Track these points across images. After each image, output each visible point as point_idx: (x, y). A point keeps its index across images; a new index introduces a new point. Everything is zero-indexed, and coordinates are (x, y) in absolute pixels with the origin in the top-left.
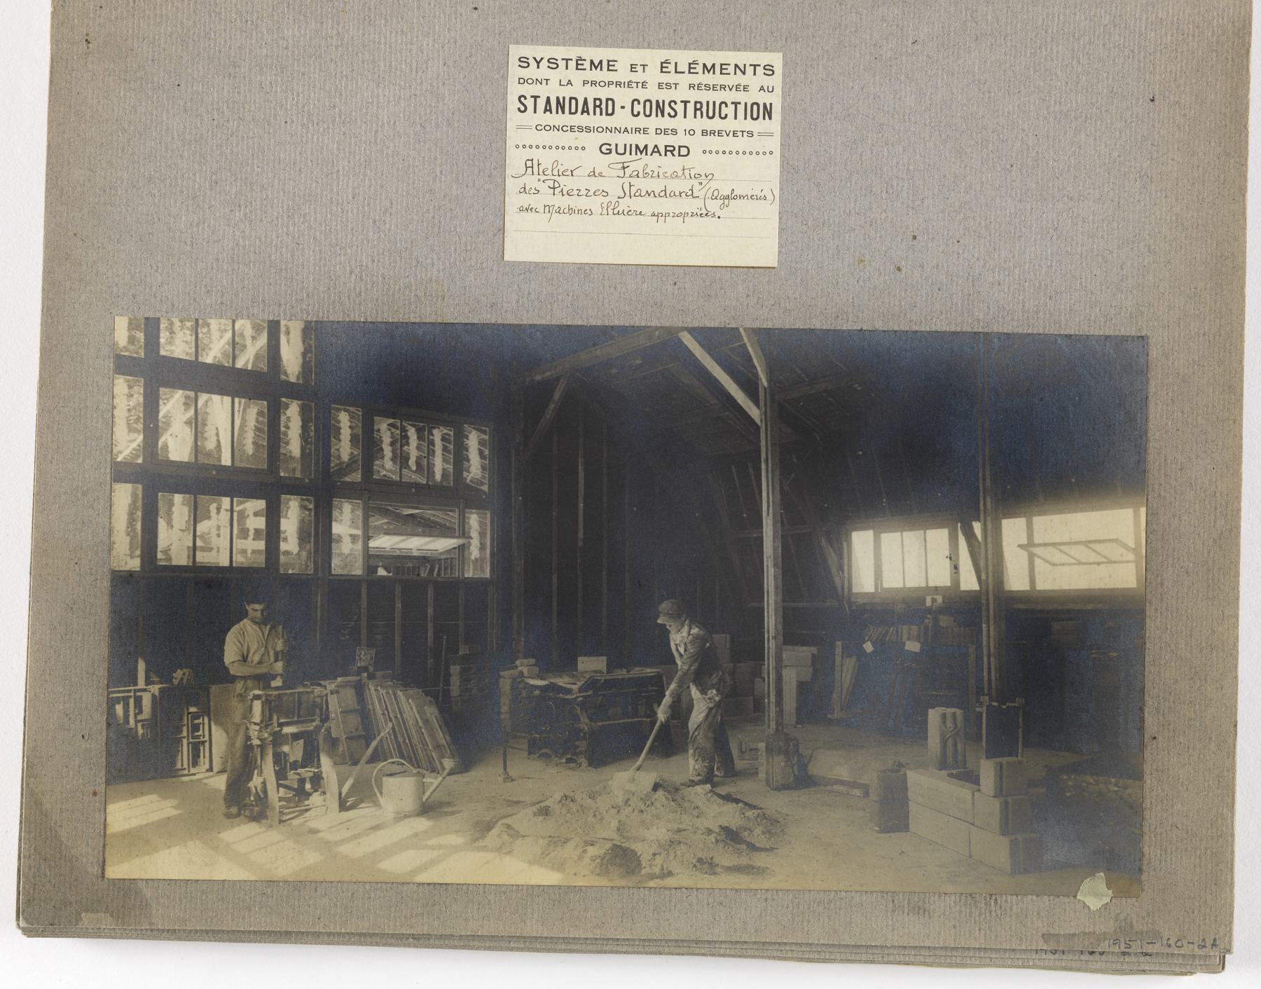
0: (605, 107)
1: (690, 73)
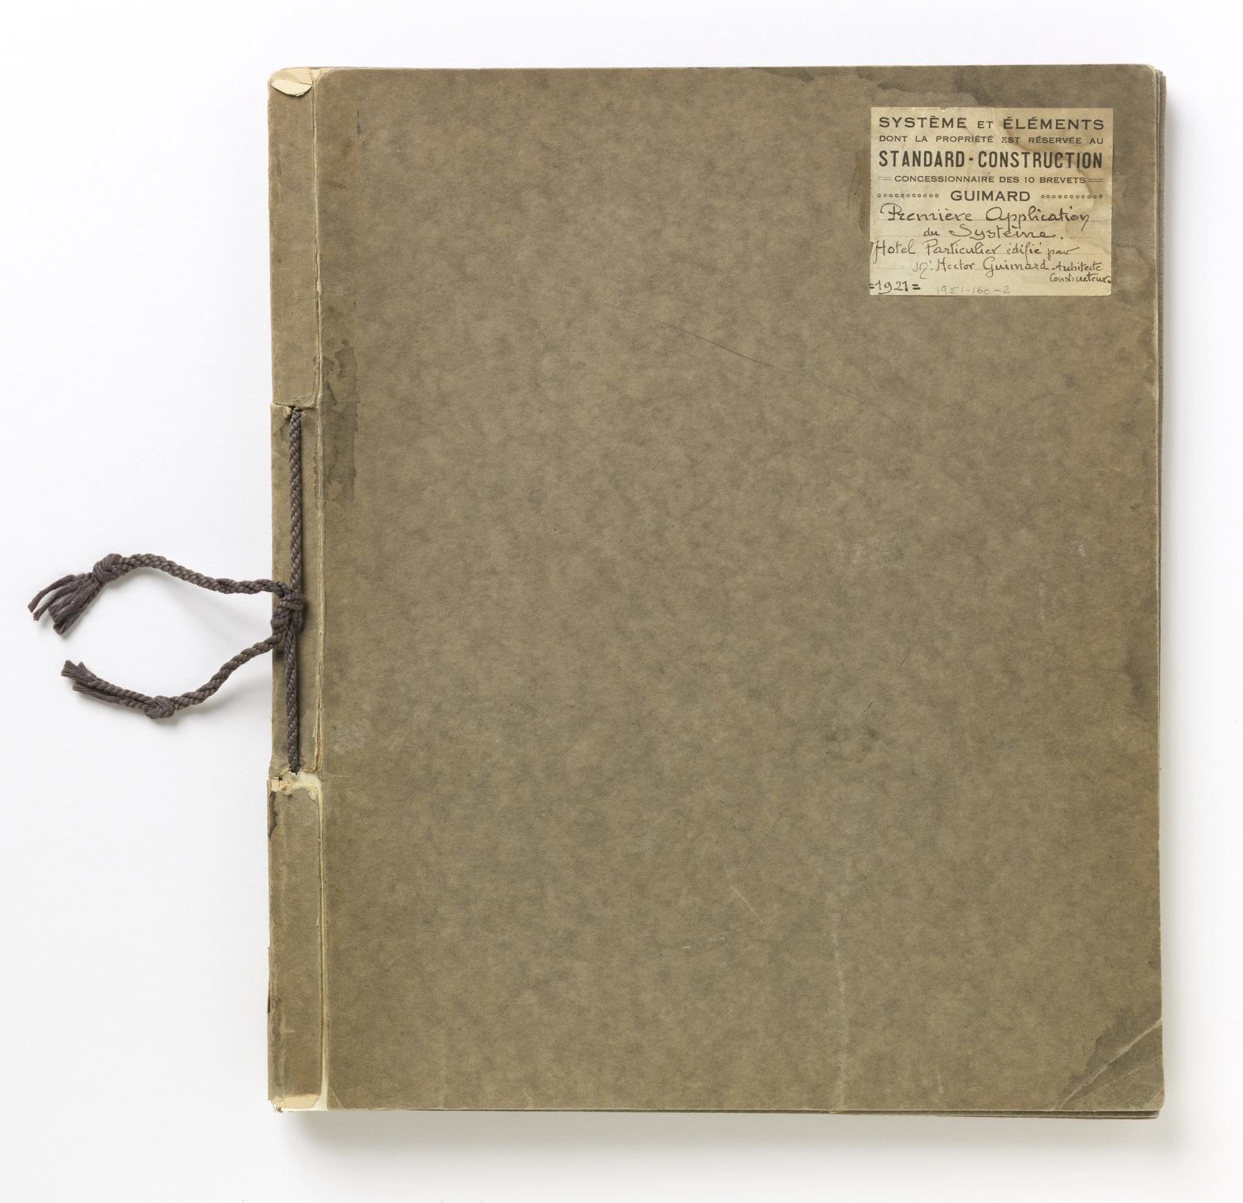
0: (957, 159)
1: (1029, 128)
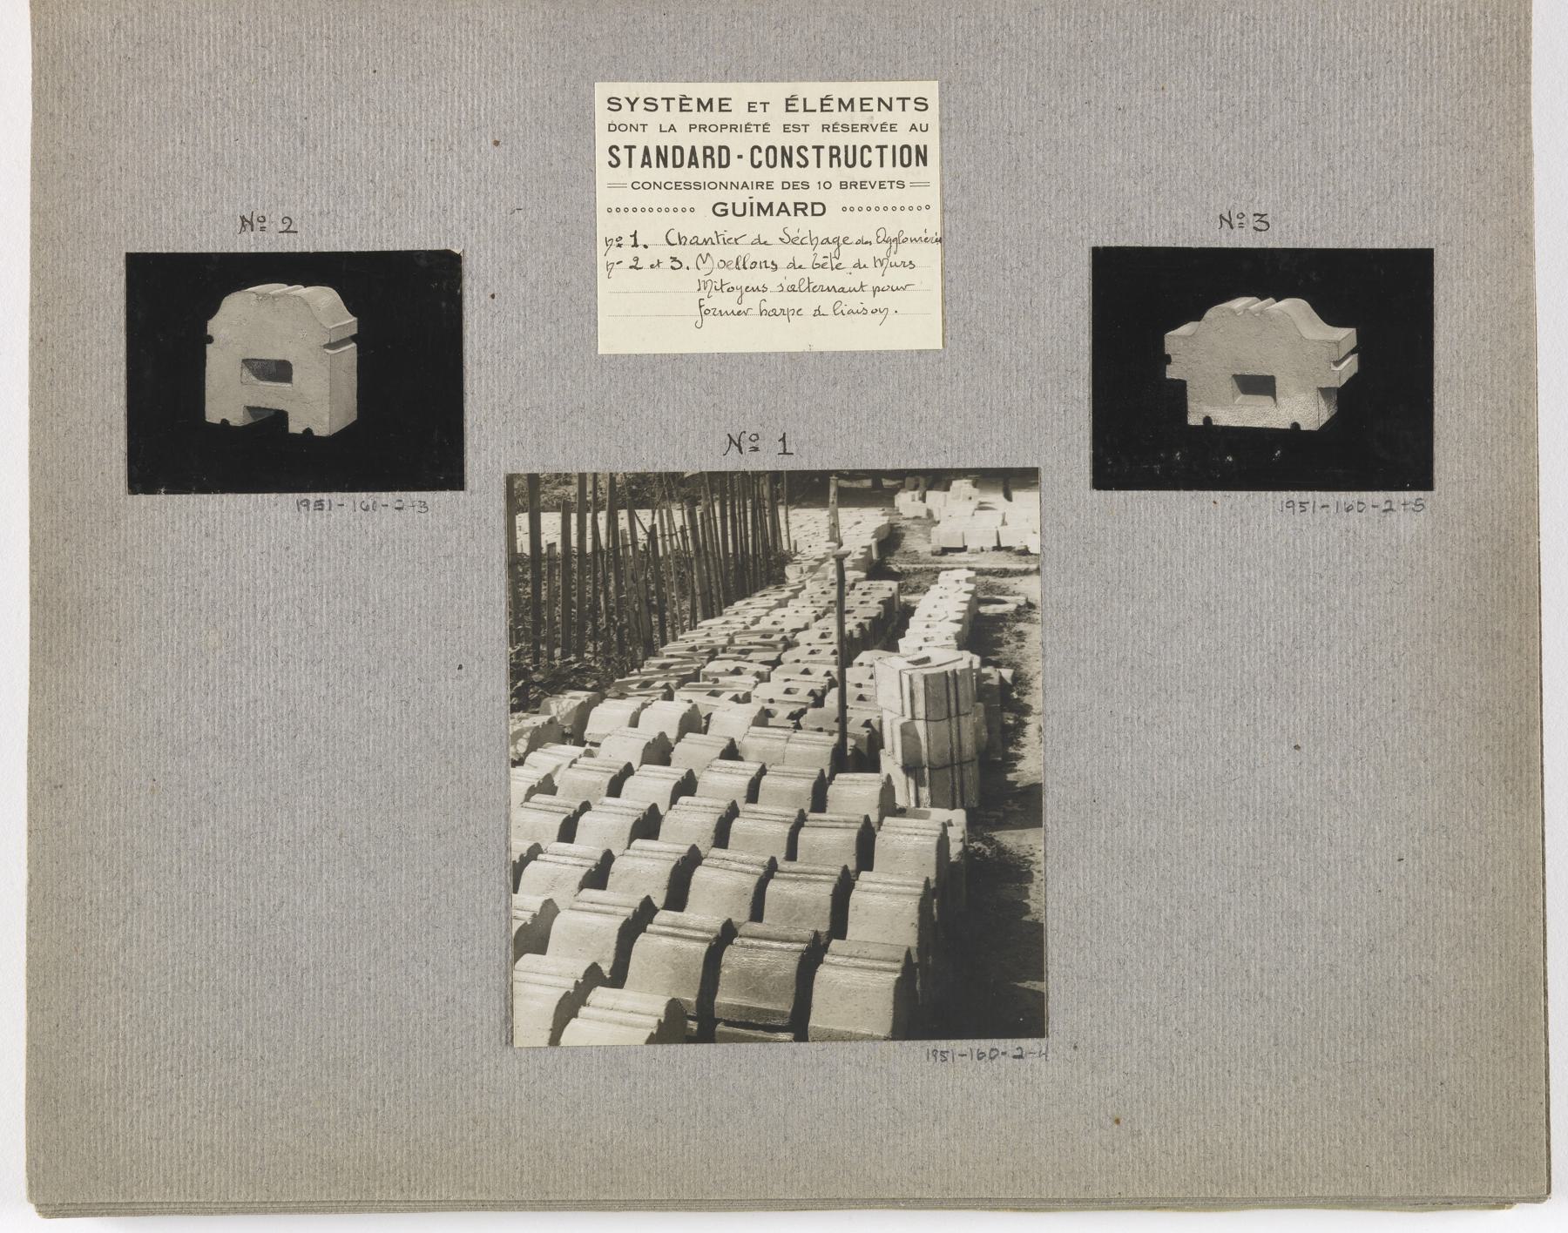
0: (718, 157)
1: (822, 110)
